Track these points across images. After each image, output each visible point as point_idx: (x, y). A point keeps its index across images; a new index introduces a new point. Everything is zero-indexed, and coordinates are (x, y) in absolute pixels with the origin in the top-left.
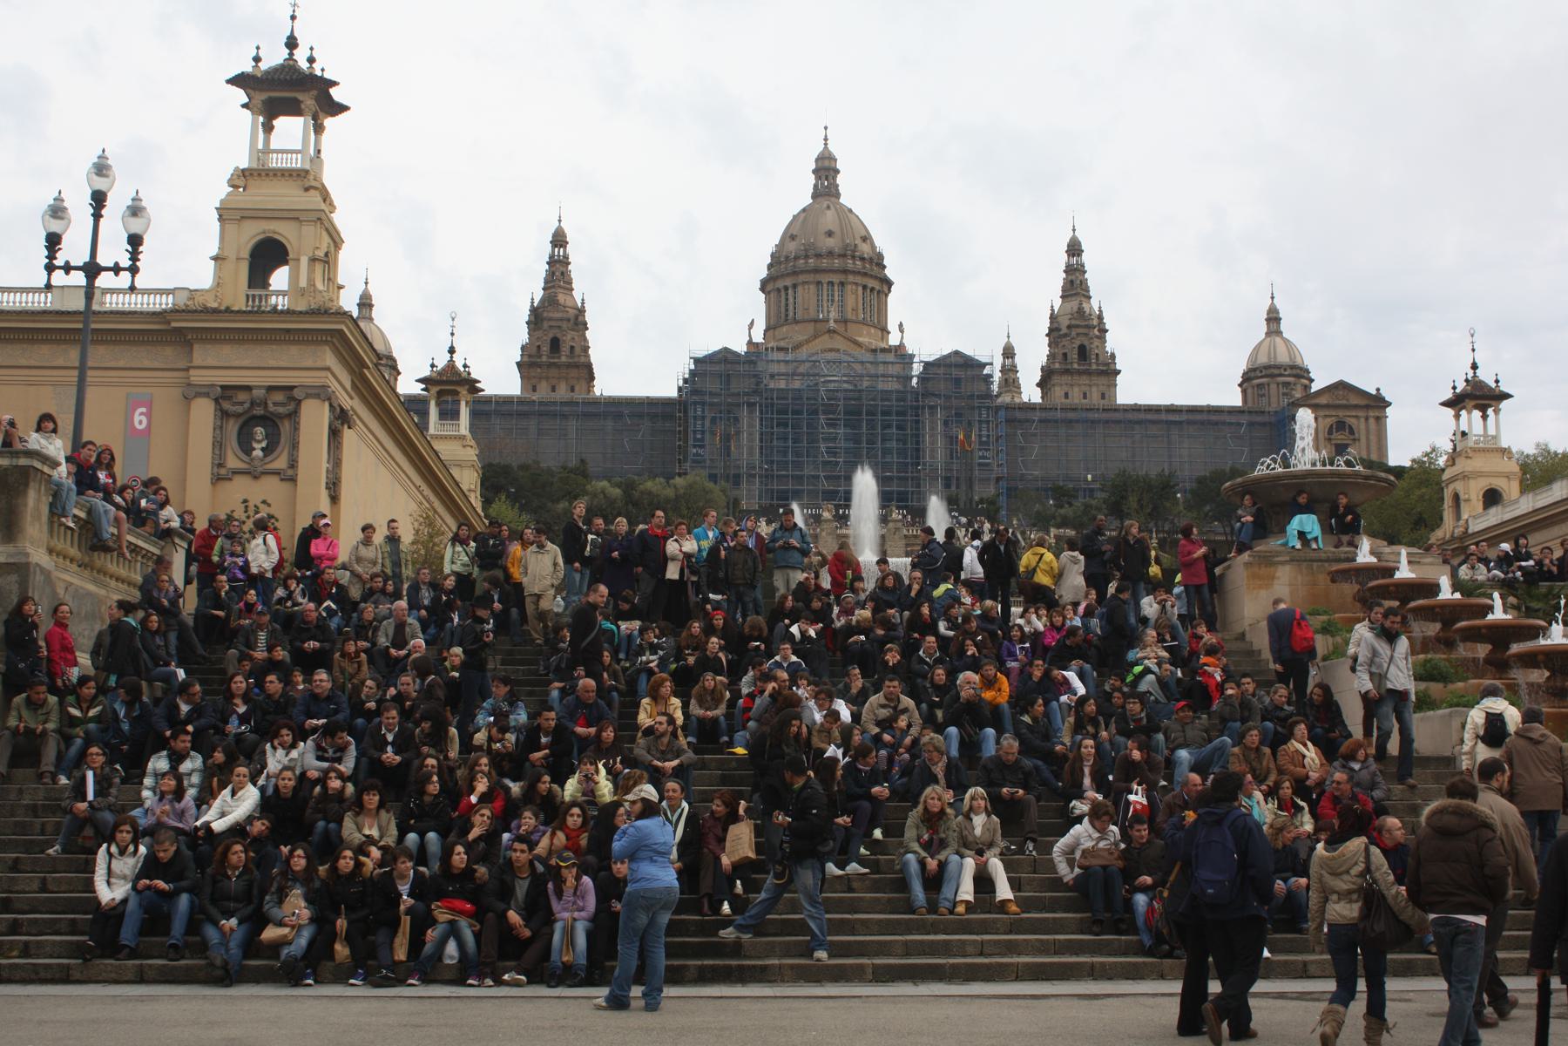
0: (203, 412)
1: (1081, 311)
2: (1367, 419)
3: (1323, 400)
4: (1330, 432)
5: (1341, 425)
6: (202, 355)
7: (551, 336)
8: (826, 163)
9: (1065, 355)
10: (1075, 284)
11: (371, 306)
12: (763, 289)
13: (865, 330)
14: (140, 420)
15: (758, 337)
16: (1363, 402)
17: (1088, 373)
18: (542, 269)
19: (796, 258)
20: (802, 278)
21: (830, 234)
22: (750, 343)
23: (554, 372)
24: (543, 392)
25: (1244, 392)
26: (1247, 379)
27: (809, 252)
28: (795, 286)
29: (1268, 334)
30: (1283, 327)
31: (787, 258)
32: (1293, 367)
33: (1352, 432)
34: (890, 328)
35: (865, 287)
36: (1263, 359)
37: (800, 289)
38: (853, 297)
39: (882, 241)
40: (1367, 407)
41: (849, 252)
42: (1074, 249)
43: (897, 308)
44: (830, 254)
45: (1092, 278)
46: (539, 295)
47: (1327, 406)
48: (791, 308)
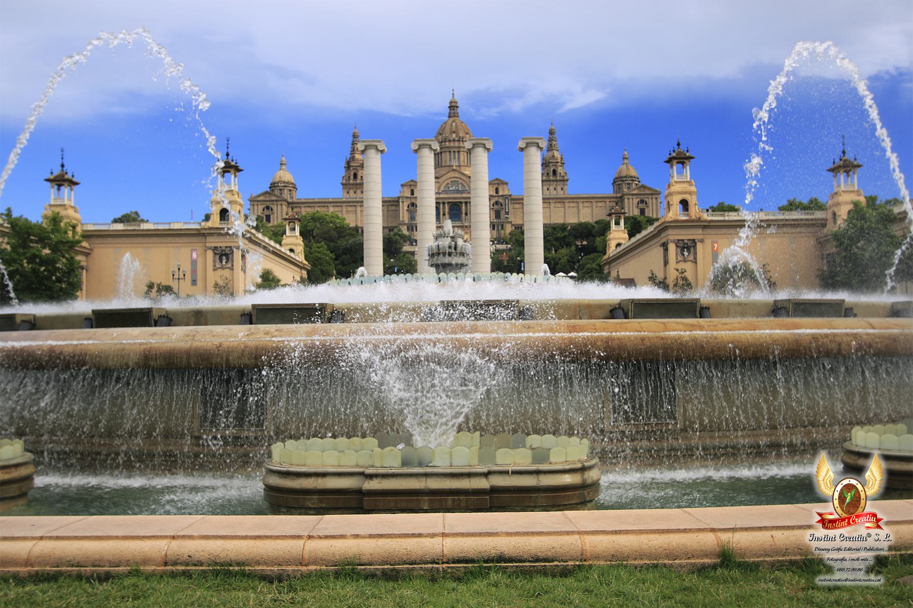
0: (210, 254)
3: (635, 192)
5: (642, 201)
6: (209, 239)
14: (194, 256)
17: (557, 181)
38: (463, 156)
40: (652, 194)
44: (454, 140)
46: (349, 156)
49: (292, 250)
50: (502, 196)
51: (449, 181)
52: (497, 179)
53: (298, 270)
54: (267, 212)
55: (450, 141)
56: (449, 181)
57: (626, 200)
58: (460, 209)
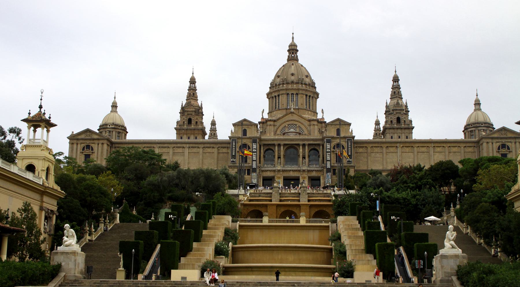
1: (398, 103)
2: (515, 143)
3: (495, 135)
4: (499, 149)
5: (503, 146)
7: (188, 117)
8: (293, 47)
9: (391, 121)
10: (396, 93)
11: (116, 107)
12: (268, 97)
13: (307, 112)
15: (266, 116)
16: (513, 136)
17: (401, 129)
18: (185, 92)
19: (279, 85)
20: (281, 92)
21: (293, 75)
22: (263, 118)
23: (189, 132)
24: (185, 139)
25: (465, 134)
26: (466, 128)
27: (285, 82)
28: (279, 96)
29: (475, 110)
30: (481, 107)
31: (276, 85)
32: (485, 123)
33: (509, 148)
34: (317, 112)
35: (306, 95)
36: (472, 120)
37: (280, 96)
39: (314, 77)
40: (515, 138)
41: (300, 82)
42: (396, 79)
43: (320, 104)
44: (292, 82)
45: (403, 91)
46: (185, 102)
47: (497, 138)
48: (277, 104)
49: (31, 168)
50: (345, 138)
51: (286, 124)
52: (338, 120)
53: (37, 196)
54: (87, 152)
55: (288, 83)
56: (286, 124)
57: (485, 144)
58: (298, 151)
